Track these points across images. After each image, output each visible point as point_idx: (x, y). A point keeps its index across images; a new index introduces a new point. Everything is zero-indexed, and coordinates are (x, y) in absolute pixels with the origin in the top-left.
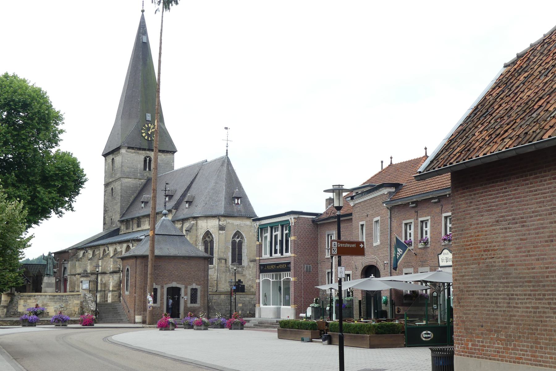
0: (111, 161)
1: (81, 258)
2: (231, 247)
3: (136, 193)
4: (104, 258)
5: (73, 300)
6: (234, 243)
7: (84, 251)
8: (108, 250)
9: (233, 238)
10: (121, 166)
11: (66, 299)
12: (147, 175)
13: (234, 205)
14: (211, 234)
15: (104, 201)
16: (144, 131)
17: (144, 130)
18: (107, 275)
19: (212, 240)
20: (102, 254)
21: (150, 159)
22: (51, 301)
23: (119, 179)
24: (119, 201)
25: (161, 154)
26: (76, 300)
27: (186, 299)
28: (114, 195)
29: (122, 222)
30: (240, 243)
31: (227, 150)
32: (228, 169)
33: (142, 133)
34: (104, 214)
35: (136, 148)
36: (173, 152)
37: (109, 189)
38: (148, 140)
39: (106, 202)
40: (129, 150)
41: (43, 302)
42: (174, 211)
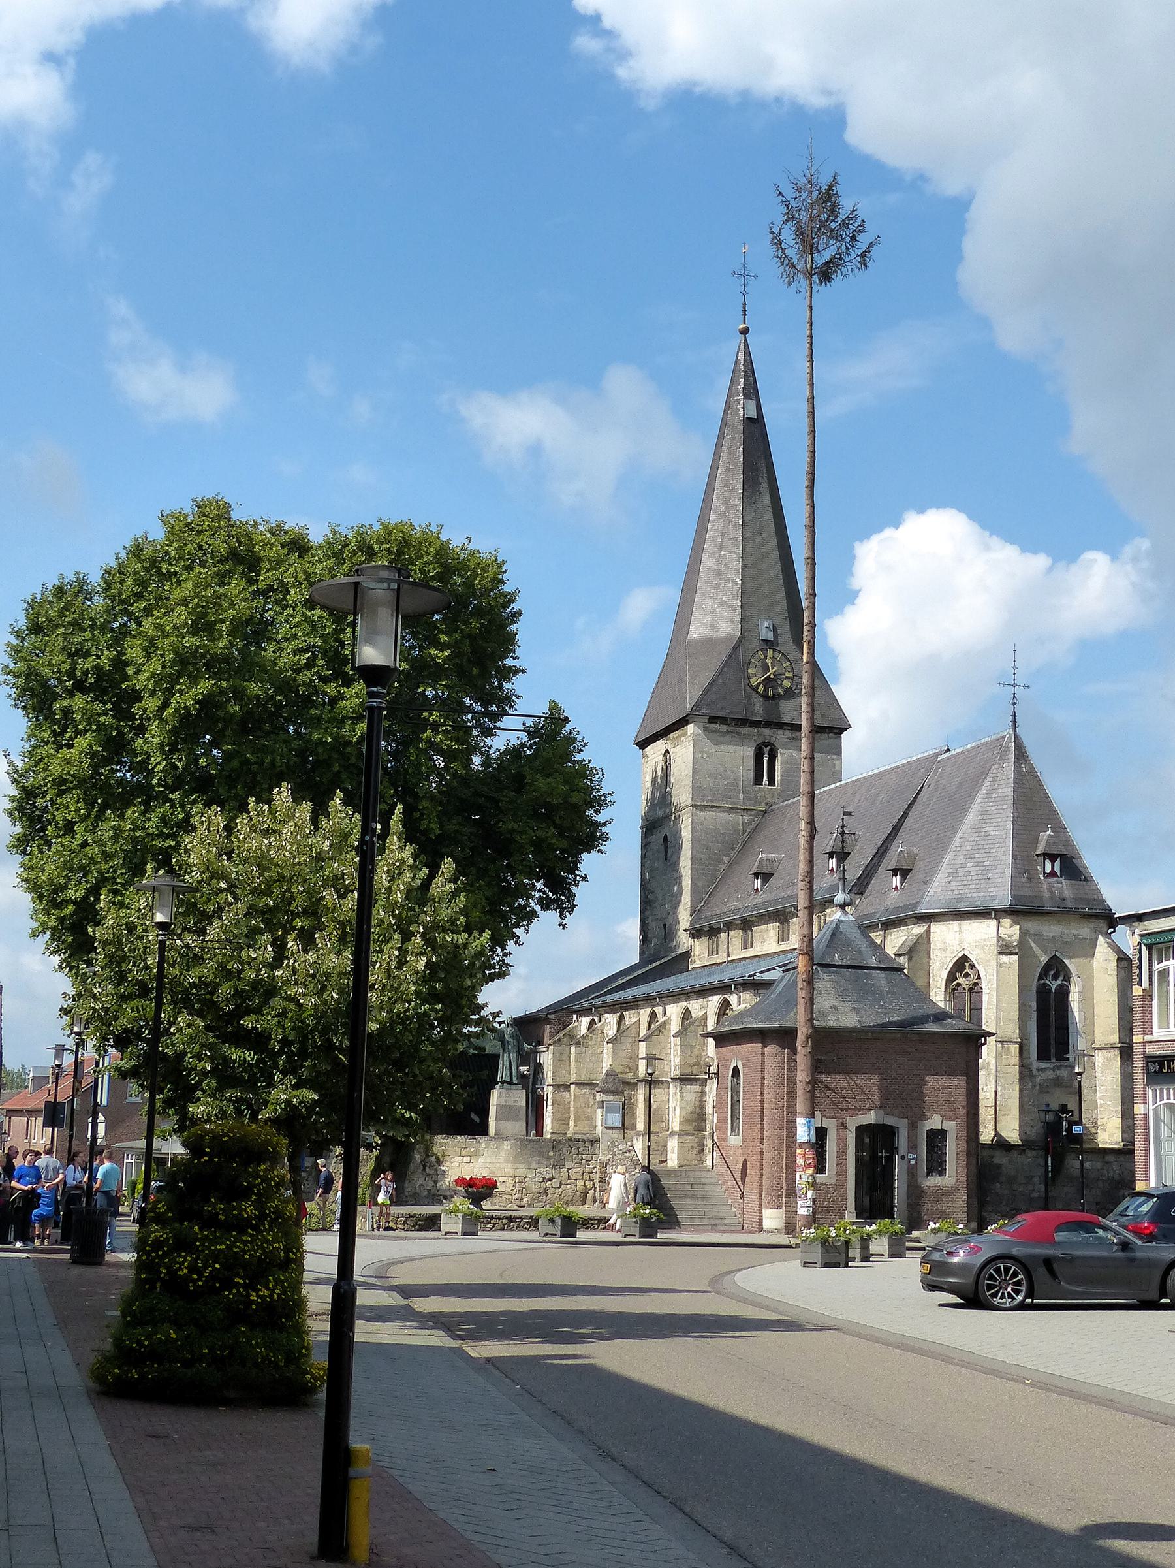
0: (661, 757)
1: (584, 1037)
2: (1034, 1004)
6: (1043, 993)
7: (591, 1018)
8: (665, 1014)
9: (1040, 978)
13: (1041, 877)
14: (973, 966)
19: (976, 984)
20: (646, 1024)
27: (912, 1162)
30: (1064, 992)
32: (1018, 770)
34: (643, 911)
37: (658, 837)
40: (713, 725)
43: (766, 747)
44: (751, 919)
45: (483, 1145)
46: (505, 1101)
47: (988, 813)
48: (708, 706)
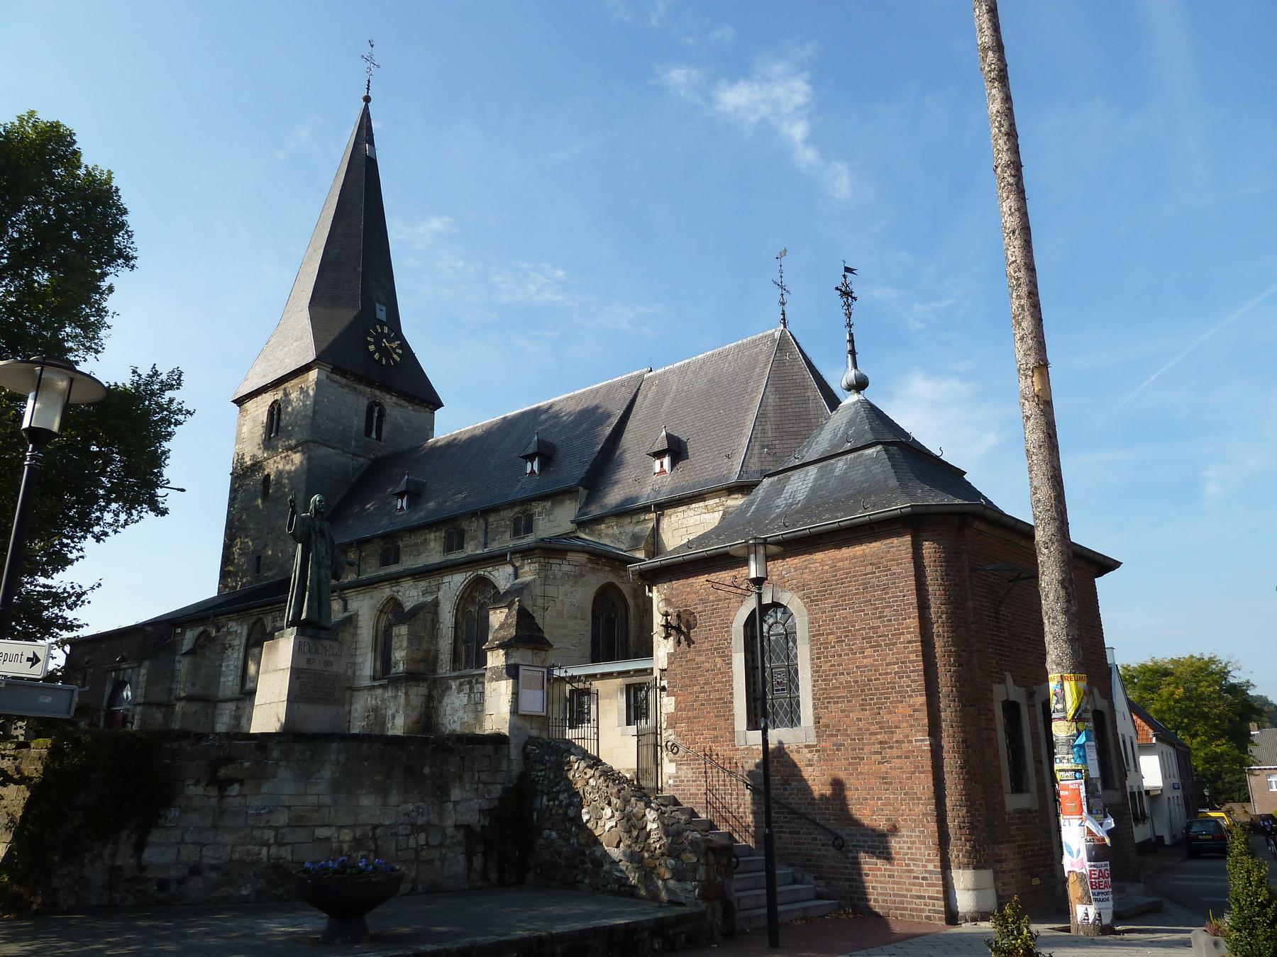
7: (201, 629)
8: (345, 609)
16: (372, 340)
25: (406, 404)
31: (783, 311)
40: (334, 376)
45: (276, 754)
46: (309, 661)
47: (788, 392)
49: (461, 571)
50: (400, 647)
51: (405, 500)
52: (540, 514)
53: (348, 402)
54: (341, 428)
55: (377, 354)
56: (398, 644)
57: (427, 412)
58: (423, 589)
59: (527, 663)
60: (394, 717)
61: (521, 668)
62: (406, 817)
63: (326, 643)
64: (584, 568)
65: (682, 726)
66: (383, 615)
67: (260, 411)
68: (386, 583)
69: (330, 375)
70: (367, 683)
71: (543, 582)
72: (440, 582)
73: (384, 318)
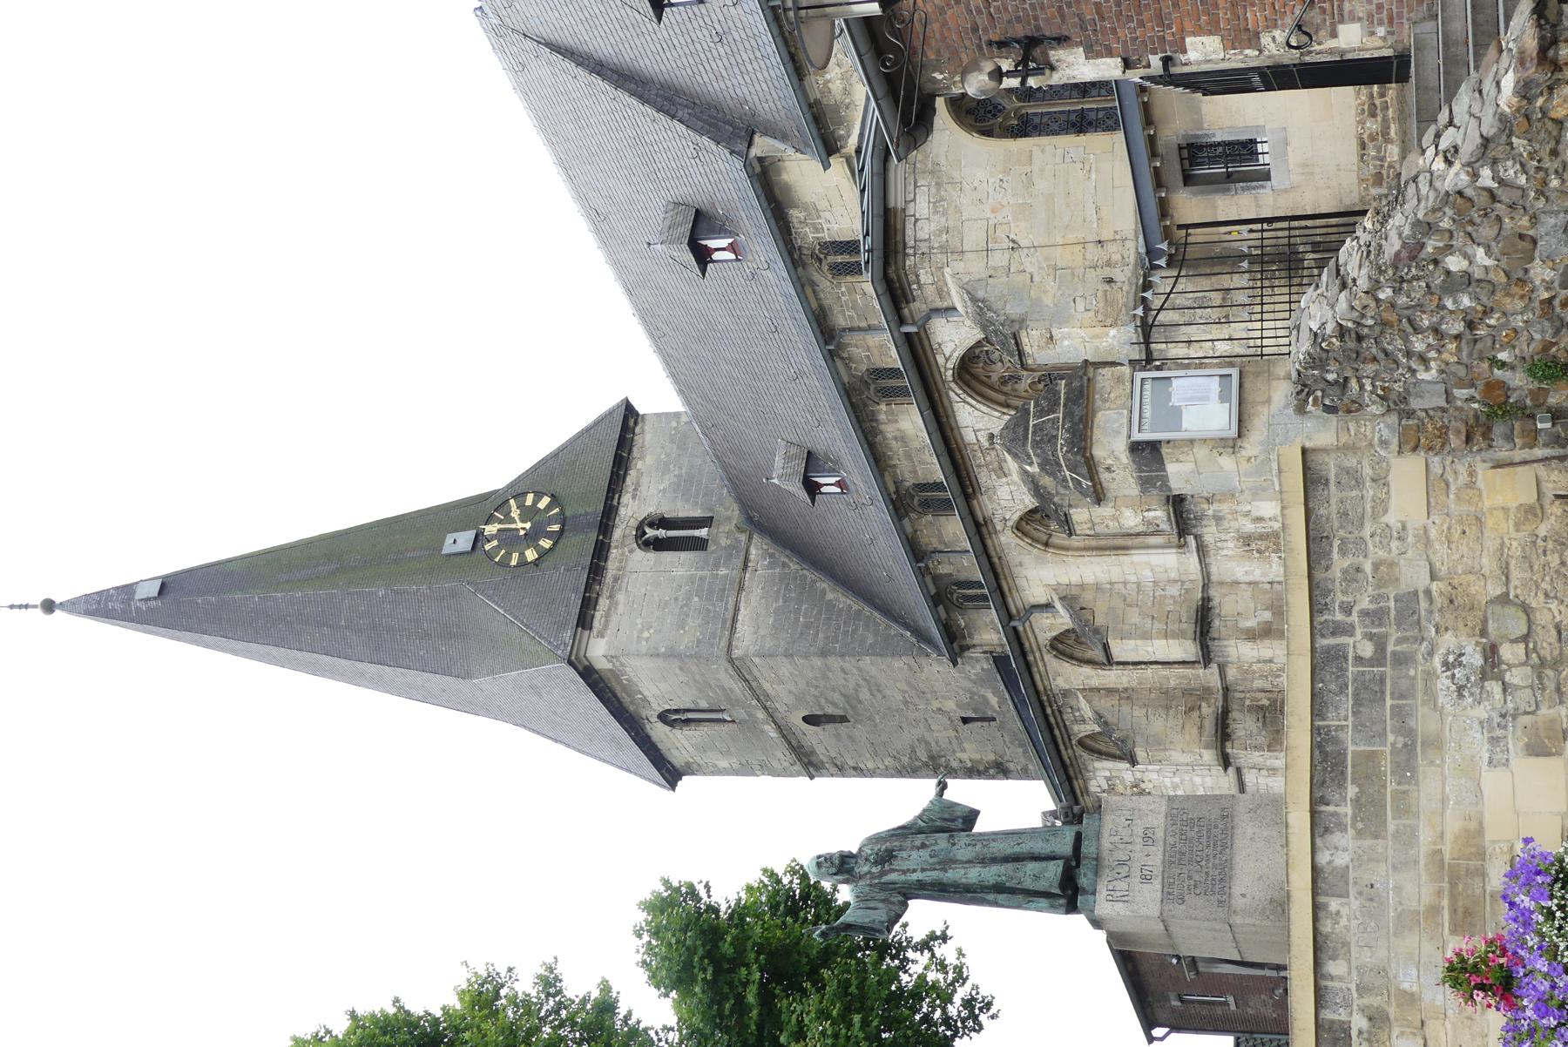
0: (677, 732)
3: (814, 582)
4: (1100, 621)
5: (1385, 533)
8: (1048, 606)
10: (675, 663)
11: (1376, 616)
12: (728, 534)
15: (888, 773)
16: (515, 556)
17: (508, 555)
18: (1215, 602)
20: (1087, 670)
21: (651, 525)
22: (1405, 808)
23: (738, 668)
24: (849, 663)
25: (632, 473)
26: (1382, 505)
28: (835, 705)
29: (955, 643)
33: (523, 563)
35: (588, 587)
36: (628, 416)
37: (814, 737)
38: (558, 537)
39: (889, 761)
40: (596, 624)
41: (1409, 921)
42: (762, 146)
43: (645, 533)
44: (892, 488)
46: (1146, 879)
48: (562, 626)
49: (950, 412)
50: (1115, 518)
51: (821, 480)
52: (817, 230)
53: (643, 591)
54: (696, 599)
55: (541, 543)
56: (1111, 524)
57: (642, 428)
58: (994, 477)
59: (1125, 421)
60: (1260, 519)
61: (1137, 437)
62: (1466, 693)
63: (1106, 843)
64: (918, 165)
65: (1253, 16)
66: (1054, 540)
67: (685, 742)
68: (989, 543)
69: (595, 631)
70: (1192, 560)
71: (956, 256)
72: (976, 447)
73: (471, 534)
